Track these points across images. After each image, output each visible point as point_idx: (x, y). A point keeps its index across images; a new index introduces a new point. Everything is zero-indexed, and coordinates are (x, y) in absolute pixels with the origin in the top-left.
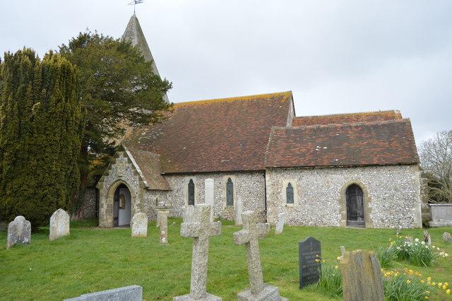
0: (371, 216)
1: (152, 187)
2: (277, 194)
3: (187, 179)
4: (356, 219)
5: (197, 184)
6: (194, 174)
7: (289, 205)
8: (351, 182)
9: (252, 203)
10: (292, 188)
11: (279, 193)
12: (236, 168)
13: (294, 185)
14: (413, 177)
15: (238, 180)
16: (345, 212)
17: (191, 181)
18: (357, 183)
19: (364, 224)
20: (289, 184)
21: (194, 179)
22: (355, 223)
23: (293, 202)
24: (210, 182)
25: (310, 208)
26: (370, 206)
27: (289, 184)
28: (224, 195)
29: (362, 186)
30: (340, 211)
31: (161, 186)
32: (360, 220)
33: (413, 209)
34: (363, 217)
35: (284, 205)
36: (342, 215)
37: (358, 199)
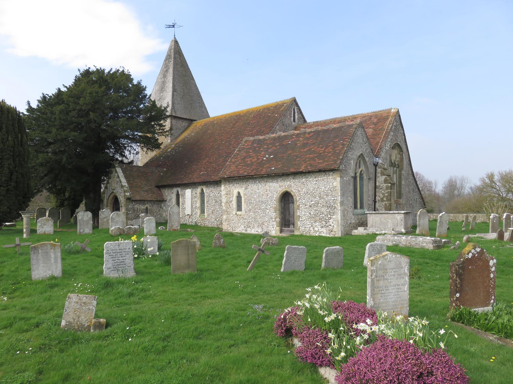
0: (299, 223)
1: (138, 198)
2: (229, 202)
3: (175, 190)
4: (288, 226)
5: (181, 195)
6: (178, 186)
7: (239, 213)
8: (284, 190)
9: (217, 211)
10: (241, 197)
11: (232, 201)
12: (207, 179)
13: (242, 195)
14: (335, 184)
15: (208, 191)
16: (278, 219)
17: (178, 192)
18: (289, 190)
19: (294, 232)
20: (239, 193)
21: (179, 190)
22: (288, 231)
23: (241, 211)
24: (188, 192)
25: (253, 216)
26: (298, 214)
27: (239, 193)
28: (198, 204)
29: (293, 194)
30: (276, 218)
31: (149, 197)
32: (291, 228)
33: (334, 217)
34: (293, 224)
35: (234, 213)
36: (277, 222)
37: (291, 205)
